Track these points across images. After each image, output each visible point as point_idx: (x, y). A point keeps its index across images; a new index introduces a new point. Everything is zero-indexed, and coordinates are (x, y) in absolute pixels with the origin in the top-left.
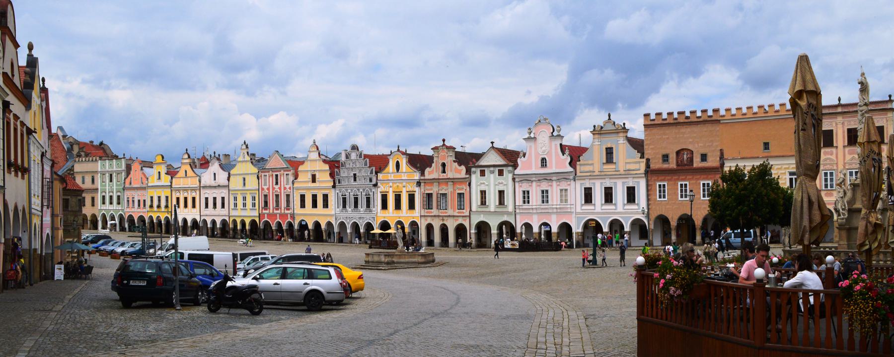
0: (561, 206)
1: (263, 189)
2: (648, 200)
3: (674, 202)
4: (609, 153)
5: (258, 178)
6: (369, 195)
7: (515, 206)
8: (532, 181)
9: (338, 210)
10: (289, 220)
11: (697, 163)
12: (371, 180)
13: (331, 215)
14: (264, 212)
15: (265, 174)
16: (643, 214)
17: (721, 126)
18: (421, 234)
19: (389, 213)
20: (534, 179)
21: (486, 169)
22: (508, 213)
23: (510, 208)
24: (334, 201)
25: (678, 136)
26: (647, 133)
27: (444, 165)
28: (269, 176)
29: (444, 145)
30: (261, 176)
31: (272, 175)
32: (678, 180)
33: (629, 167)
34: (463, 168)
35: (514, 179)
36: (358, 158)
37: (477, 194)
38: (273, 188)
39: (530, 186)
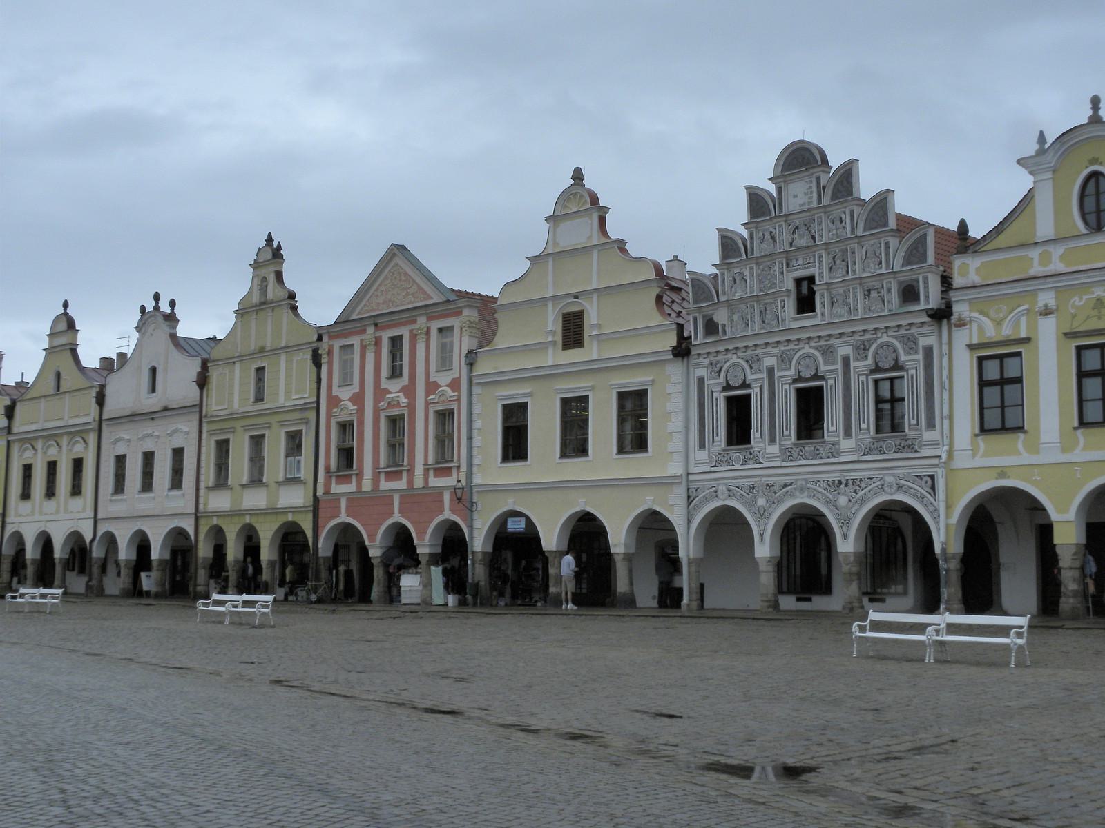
1: (334, 401)
5: (316, 360)
6: (897, 366)
9: (703, 455)
10: (447, 515)
12: (910, 293)
13: (666, 483)
14: (336, 488)
15: (348, 342)
19: (1034, 448)
24: (678, 417)
28: (363, 348)
30: (330, 353)
31: (378, 342)
36: (826, 200)
38: (380, 393)
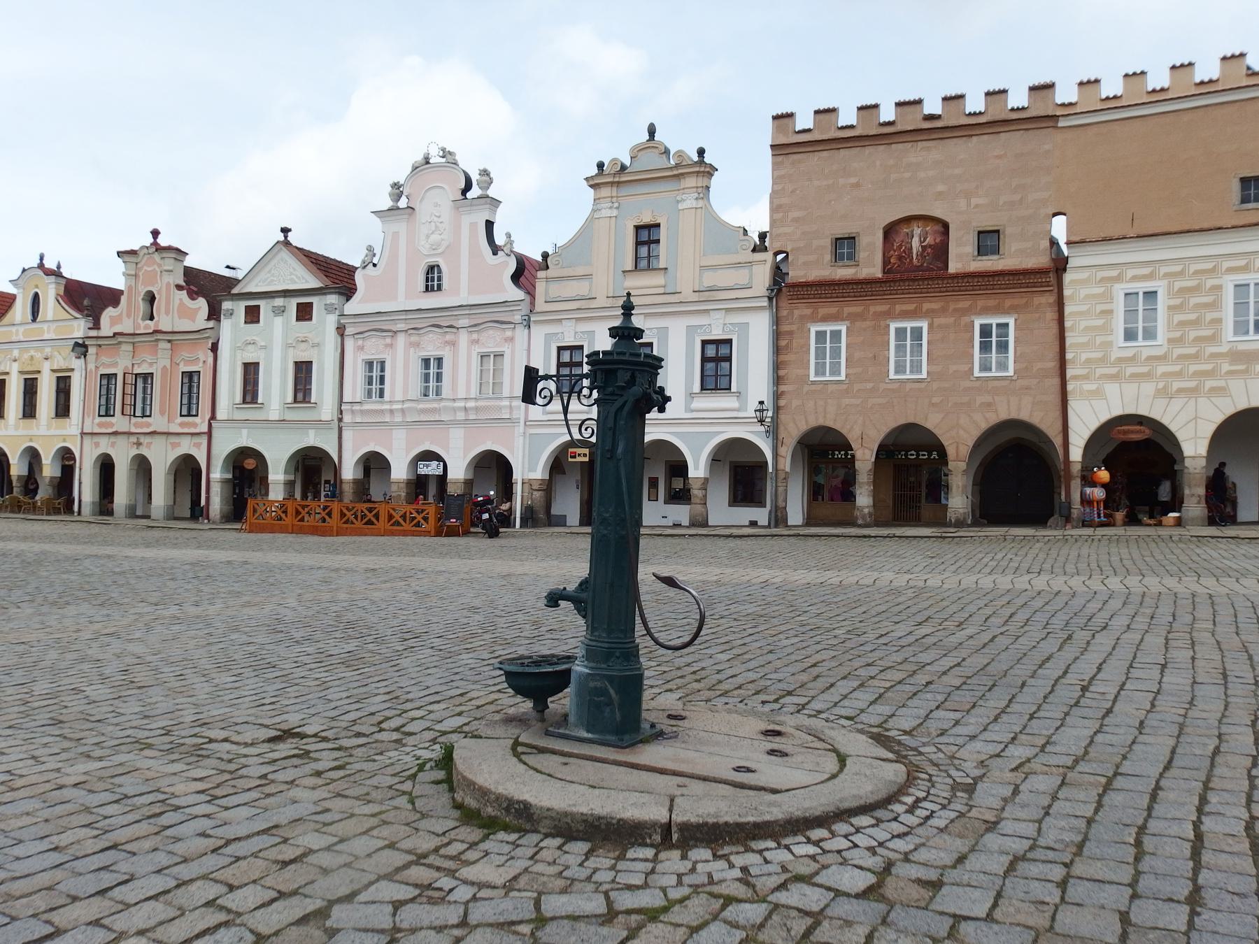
0: (480, 403)
2: (777, 380)
3: (869, 386)
4: (643, 243)
7: (341, 401)
8: (395, 332)
11: (961, 257)
16: (761, 421)
17: (1058, 137)
18: (80, 483)
20: (401, 326)
21: (262, 303)
22: (319, 424)
23: (327, 410)
25: (893, 176)
26: (783, 172)
27: (151, 298)
29: (155, 244)
32: (890, 315)
33: (710, 280)
34: (202, 304)
35: (341, 330)
37: (233, 372)
39: (387, 346)
